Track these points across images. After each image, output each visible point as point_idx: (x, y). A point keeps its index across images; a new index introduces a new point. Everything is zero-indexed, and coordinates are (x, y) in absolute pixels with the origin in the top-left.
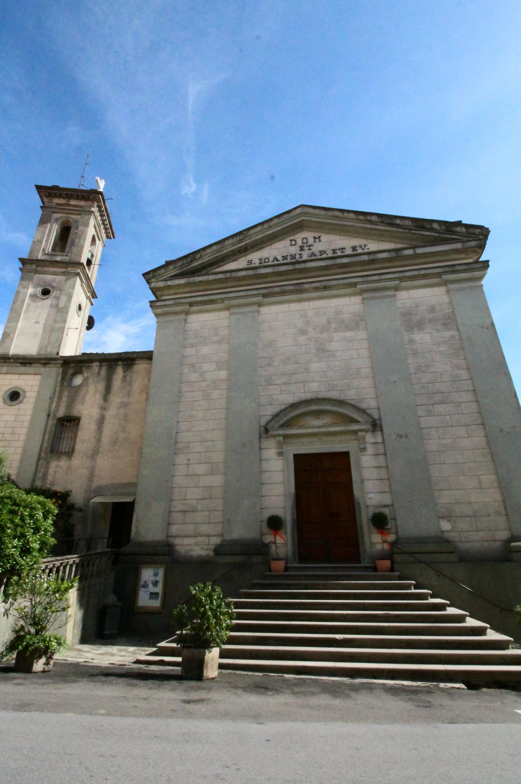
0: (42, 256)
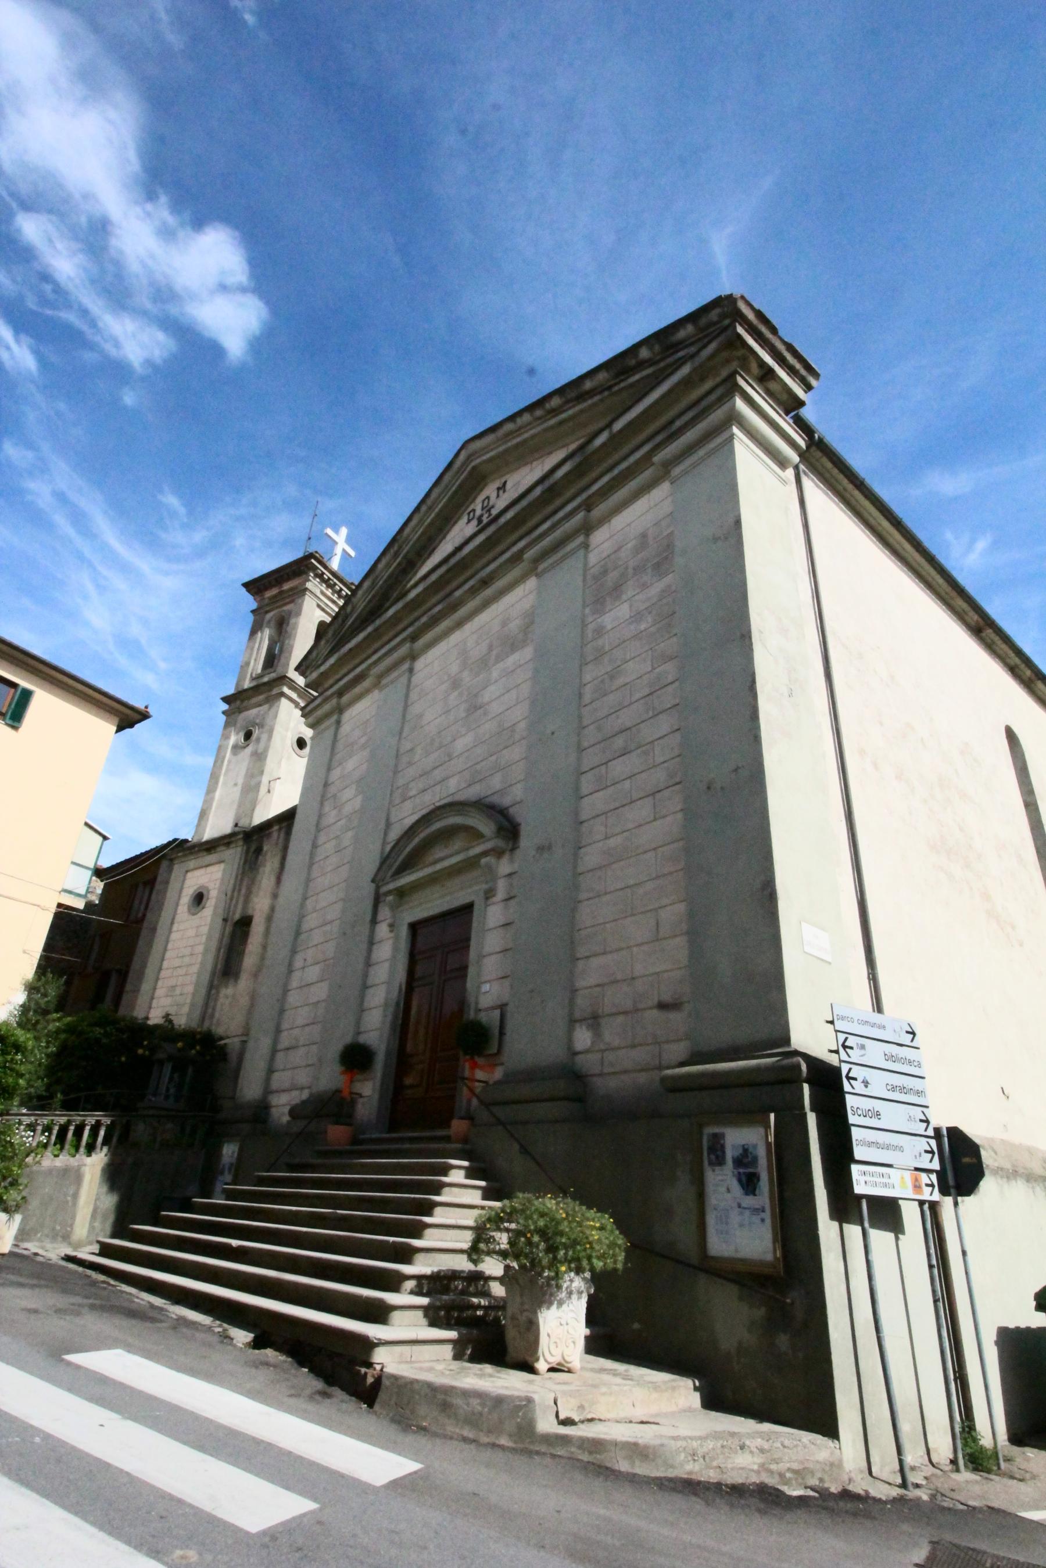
0: (250, 683)
